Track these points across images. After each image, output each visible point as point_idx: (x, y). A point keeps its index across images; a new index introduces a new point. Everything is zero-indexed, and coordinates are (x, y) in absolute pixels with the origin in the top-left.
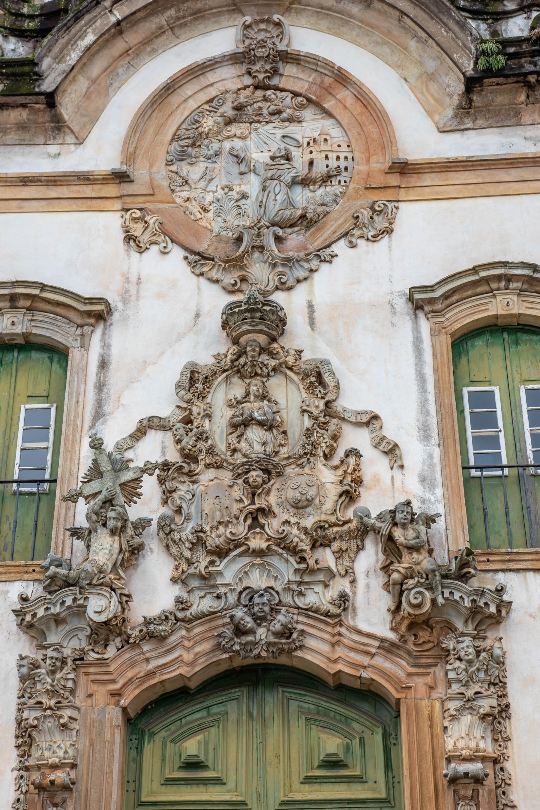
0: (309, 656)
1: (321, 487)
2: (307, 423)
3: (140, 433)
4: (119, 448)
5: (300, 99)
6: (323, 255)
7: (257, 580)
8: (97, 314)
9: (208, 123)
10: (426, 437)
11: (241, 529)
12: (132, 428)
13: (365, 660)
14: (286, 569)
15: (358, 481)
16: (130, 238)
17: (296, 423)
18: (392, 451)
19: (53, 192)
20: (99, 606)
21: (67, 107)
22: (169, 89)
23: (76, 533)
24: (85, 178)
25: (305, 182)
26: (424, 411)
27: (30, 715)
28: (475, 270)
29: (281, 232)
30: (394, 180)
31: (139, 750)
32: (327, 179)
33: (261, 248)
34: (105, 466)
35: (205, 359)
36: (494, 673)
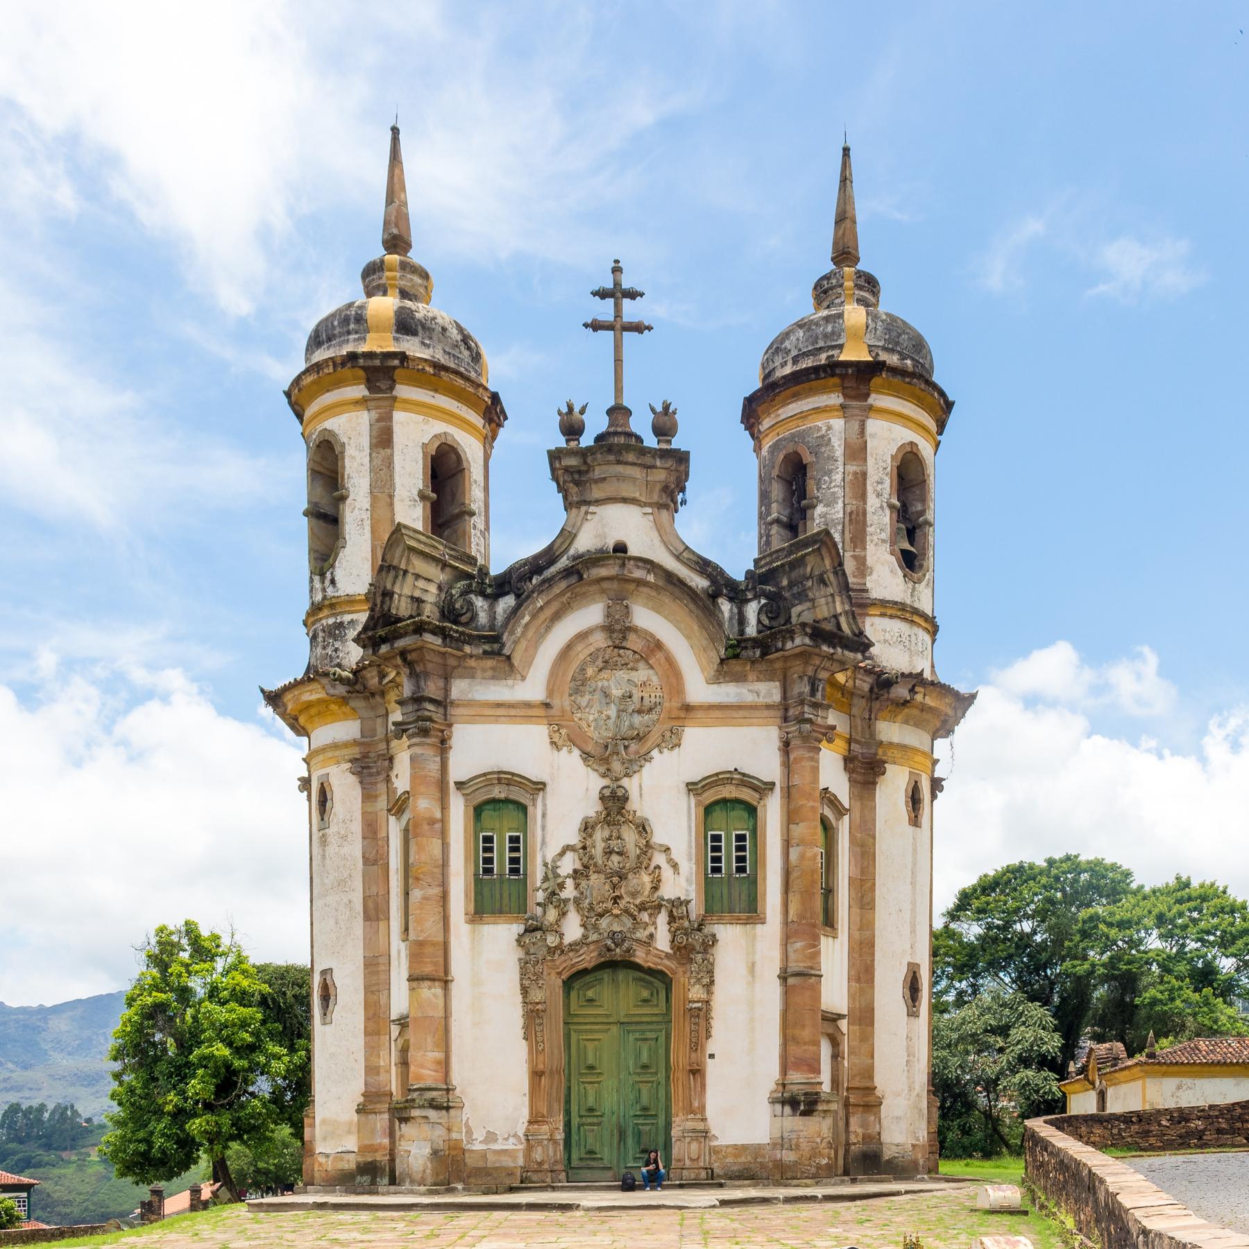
0: (637, 960)
1: (643, 884)
2: (638, 851)
3: (562, 854)
4: (554, 861)
5: (637, 656)
7: (616, 928)
10: (690, 860)
11: (609, 904)
12: (559, 850)
13: (658, 961)
14: (629, 923)
15: (659, 881)
17: (633, 851)
18: (675, 866)
20: (552, 940)
21: (516, 661)
22: (569, 647)
23: (538, 904)
26: (690, 846)
27: (527, 983)
28: (717, 774)
29: (626, 743)
30: (682, 714)
31: (569, 994)
34: (550, 875)
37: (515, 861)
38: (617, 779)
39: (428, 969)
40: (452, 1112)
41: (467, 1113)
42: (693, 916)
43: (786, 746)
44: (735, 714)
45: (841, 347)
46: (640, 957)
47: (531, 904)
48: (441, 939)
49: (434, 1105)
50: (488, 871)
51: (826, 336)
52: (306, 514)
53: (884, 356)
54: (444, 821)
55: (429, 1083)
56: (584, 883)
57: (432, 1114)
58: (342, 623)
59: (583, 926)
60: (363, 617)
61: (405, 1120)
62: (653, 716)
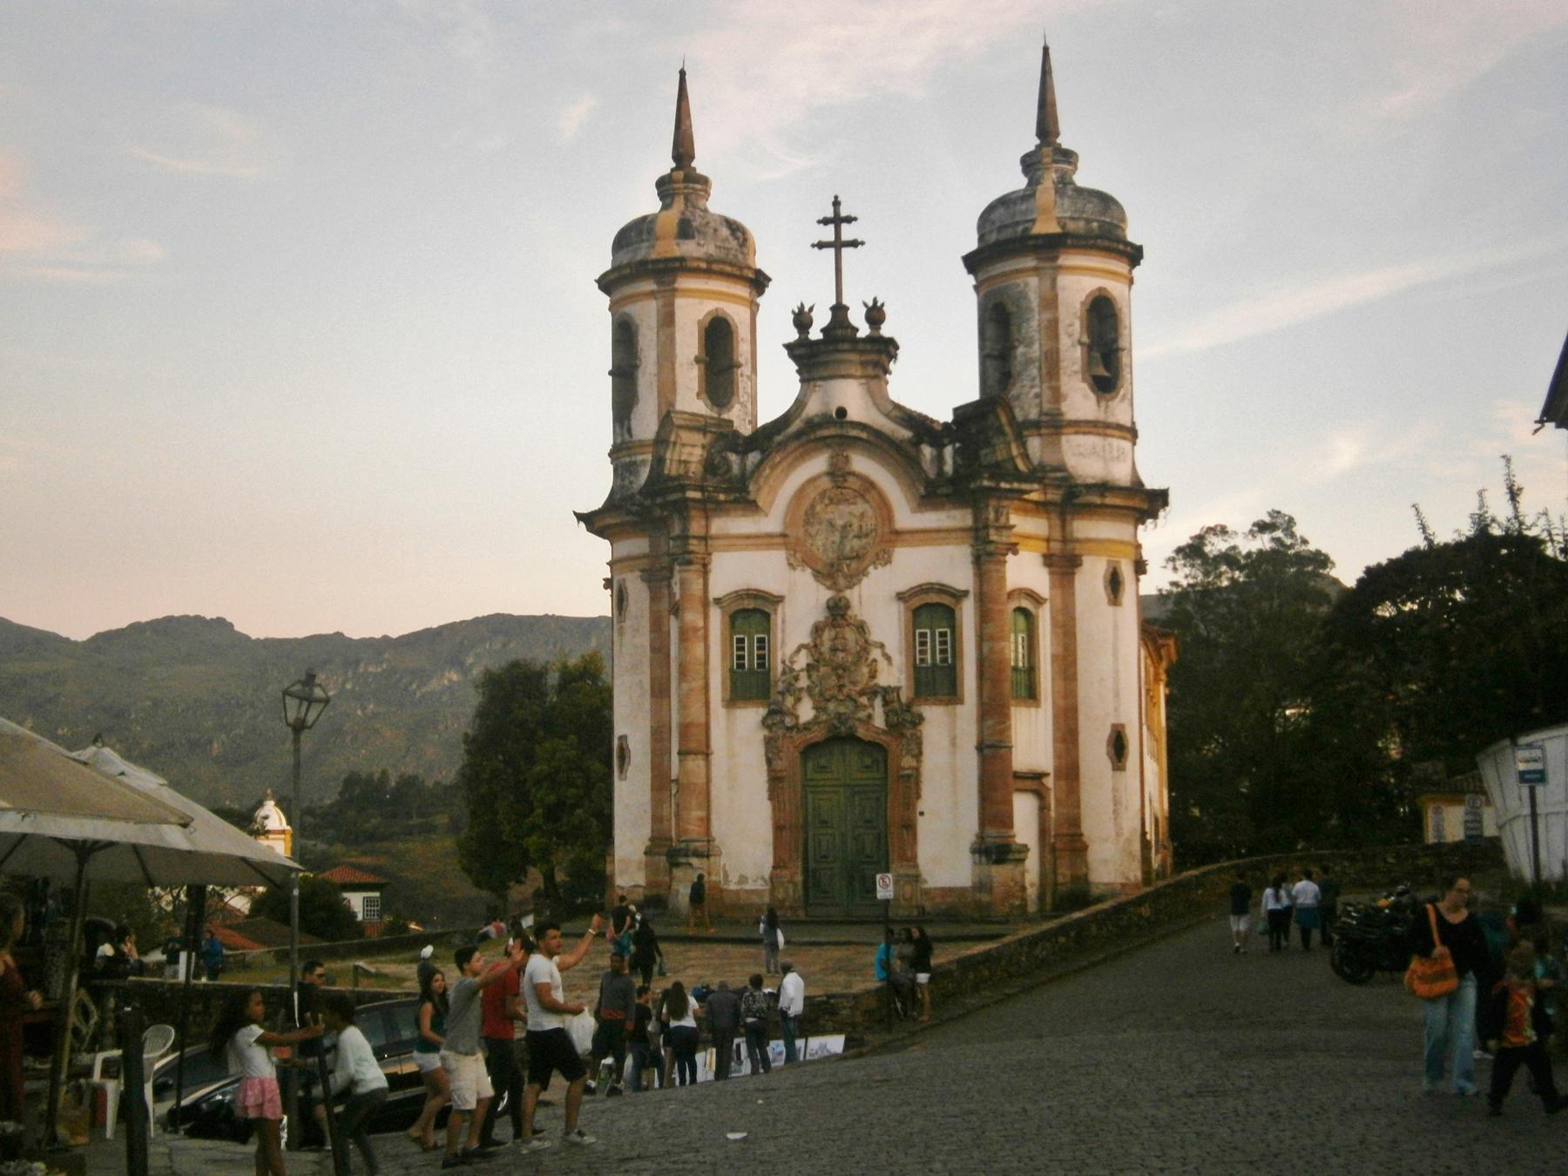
3: (798, 651)
6: (864, 572)
7: (842, 710)
8: (779, 600)
9: (818, 508)
14: (850, 704)
16: (790, 564)
19: (759, 541)
20: (789, 721)
24: (770, 536)
25: (858, 537)
30: (893, 537)
32: (867, 535)
33: (840, 570)
35: (821, 618)
36: (919, 743)
37: (761, 657)
38: (840, 591)
39: (693, 745)
40: (712, 859)
41: (723, 860)
42: (904, 699)
43: (978, 561)
44: (935, 535)
45: (1033, 221)
46: (861, 732)
47: (773, 691)
48: (703, 720)
49: (697, 854)
50: (741, 666)
51: (1022, 213)
52: (610, 373)
53: (1071, 226)
54: (706, 628)
55: (694, 836)
56: (814, 675)
57: (695, 861)
58: (635, 463)
59: (816, 708)
60: (649, 457)
61: (678, 865)
62: (870, 540)
